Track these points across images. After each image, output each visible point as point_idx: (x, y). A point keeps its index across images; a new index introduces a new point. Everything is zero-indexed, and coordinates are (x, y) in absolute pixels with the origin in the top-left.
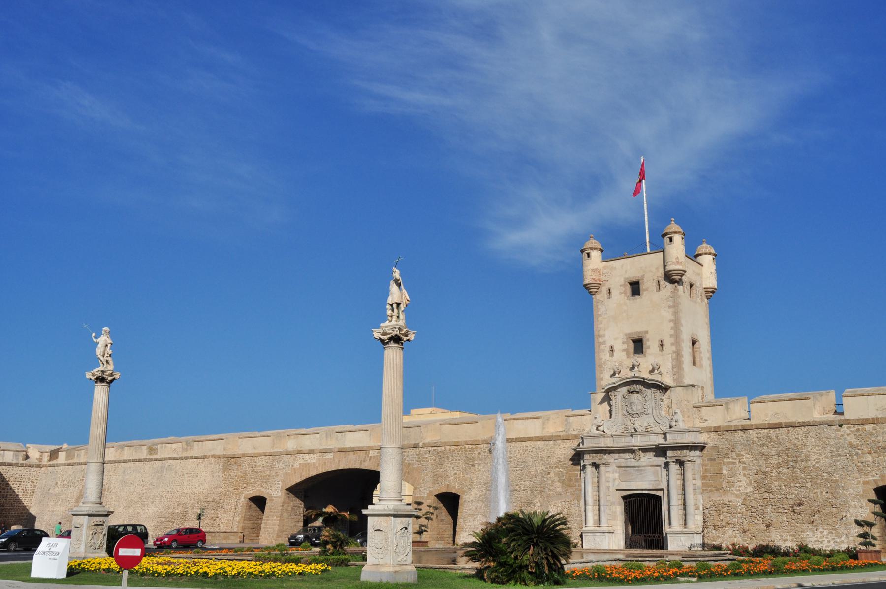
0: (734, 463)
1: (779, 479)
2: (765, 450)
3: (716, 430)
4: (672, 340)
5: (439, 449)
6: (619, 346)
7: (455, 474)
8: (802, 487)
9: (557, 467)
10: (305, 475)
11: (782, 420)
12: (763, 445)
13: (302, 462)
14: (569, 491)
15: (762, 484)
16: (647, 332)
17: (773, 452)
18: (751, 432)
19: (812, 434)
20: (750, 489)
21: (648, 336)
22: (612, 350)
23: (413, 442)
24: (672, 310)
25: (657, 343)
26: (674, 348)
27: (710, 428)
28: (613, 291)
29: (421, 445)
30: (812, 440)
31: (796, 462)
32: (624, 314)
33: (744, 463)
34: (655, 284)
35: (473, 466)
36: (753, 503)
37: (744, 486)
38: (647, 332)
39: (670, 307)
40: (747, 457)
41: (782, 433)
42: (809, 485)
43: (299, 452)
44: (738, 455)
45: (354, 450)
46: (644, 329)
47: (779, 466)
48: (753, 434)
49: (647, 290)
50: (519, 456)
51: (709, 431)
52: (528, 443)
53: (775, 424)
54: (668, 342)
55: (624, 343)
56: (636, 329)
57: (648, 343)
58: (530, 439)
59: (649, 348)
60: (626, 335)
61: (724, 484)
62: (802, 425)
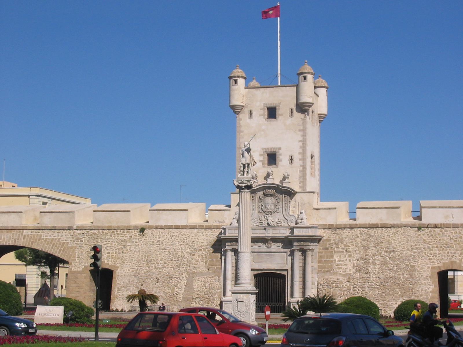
9: (200, 250)
16: (280, 149)
21: (281, 152)
24: (301, 133)
28: (254, 113)
32: (262, 133)
34: (289, 111)
35: (125, 247)
38: (280, 149)
39: (300, 130)
46: (278, 146)
49: (282, 115)
50: (167, 240)
54: (297, 158)
55: (261, 155)
56: (271, 145)
57: (281, 157)
59: (281, 161)
60: (263, 149)
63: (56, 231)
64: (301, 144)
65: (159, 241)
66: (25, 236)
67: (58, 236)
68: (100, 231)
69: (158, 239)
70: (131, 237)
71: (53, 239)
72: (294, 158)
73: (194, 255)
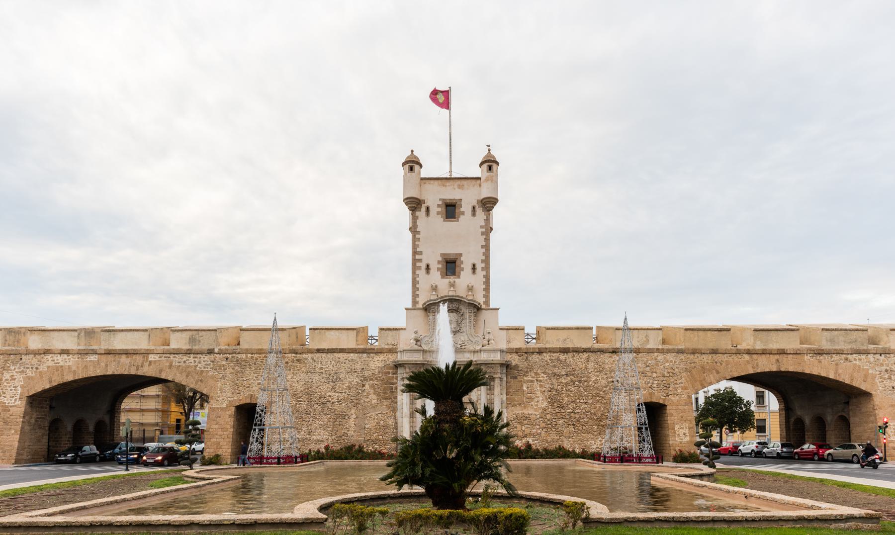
0: (532, 381)
1: (568, 396)
2: (556, 371)
3: (517, 351)
4: (483, 265)
5: (239, 356)
6: (434, 266)
7: (259, 384)
8: (585, 403)
10: (57, 380)
11: (570, 345)
12: (554, 366)
13: (51, 363)
14: (385, 403)
15: (554, 401)
16: (461, 255)
17: (563, 373)
18: (545, 354)
19: (592, 359)
20: (545, 404)
21: (462, 259)
22: (428, 268)
23: (206, 347)
25: (471, 266)
26: (484, 273)
27: (512, 349)
29: (216, 350)
30: (591, 365)
31: (580, 382)
33: (541, 381)
34: (470, 209)
36: (549, 417)
37: (541, 402)
38: (461, 255)
40: (543, 377)
41: (569, 357)
42: (590, 401)
43: (47, 352)
44: (536, 374)
45: (127, 353)
47: (567, 385)
48: (547, 356)
51: (511, 351)
52: (340, 355)
53: (564, 349)
54: (479, 266)
58: (342, 351)
59: (463, 269)
61: (525, 399)
62: (585, 351)
63: (192, 356)
64: (484, 250)
65: (321, 368)
66: (150, 362)
67: (195, 362)
68: (249, 355)
69: (319, 366)
70: (287, 363)
71: (189, 367)
72: (431, 267)
73: (364, 386)
